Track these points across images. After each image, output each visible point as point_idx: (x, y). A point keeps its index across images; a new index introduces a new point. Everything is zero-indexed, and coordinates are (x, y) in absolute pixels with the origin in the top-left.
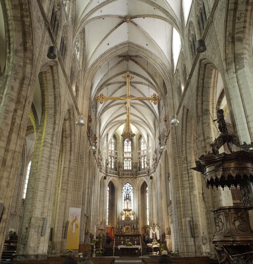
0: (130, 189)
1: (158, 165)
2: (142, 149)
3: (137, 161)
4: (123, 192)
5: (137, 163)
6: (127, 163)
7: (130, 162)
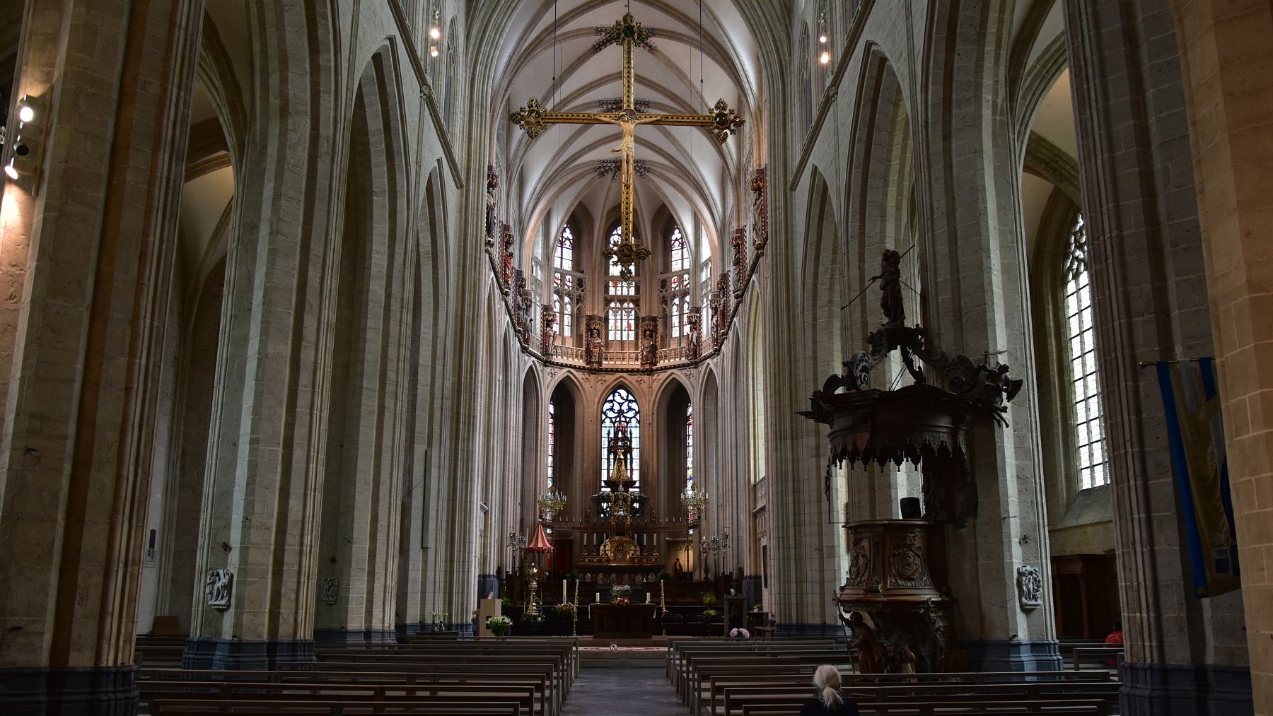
0: (630, 409)
1: (731, 333)
2: (676, 266)
4: (603, 422)
5: (654, 319)
6: (619, 317)
7: (628, 316)
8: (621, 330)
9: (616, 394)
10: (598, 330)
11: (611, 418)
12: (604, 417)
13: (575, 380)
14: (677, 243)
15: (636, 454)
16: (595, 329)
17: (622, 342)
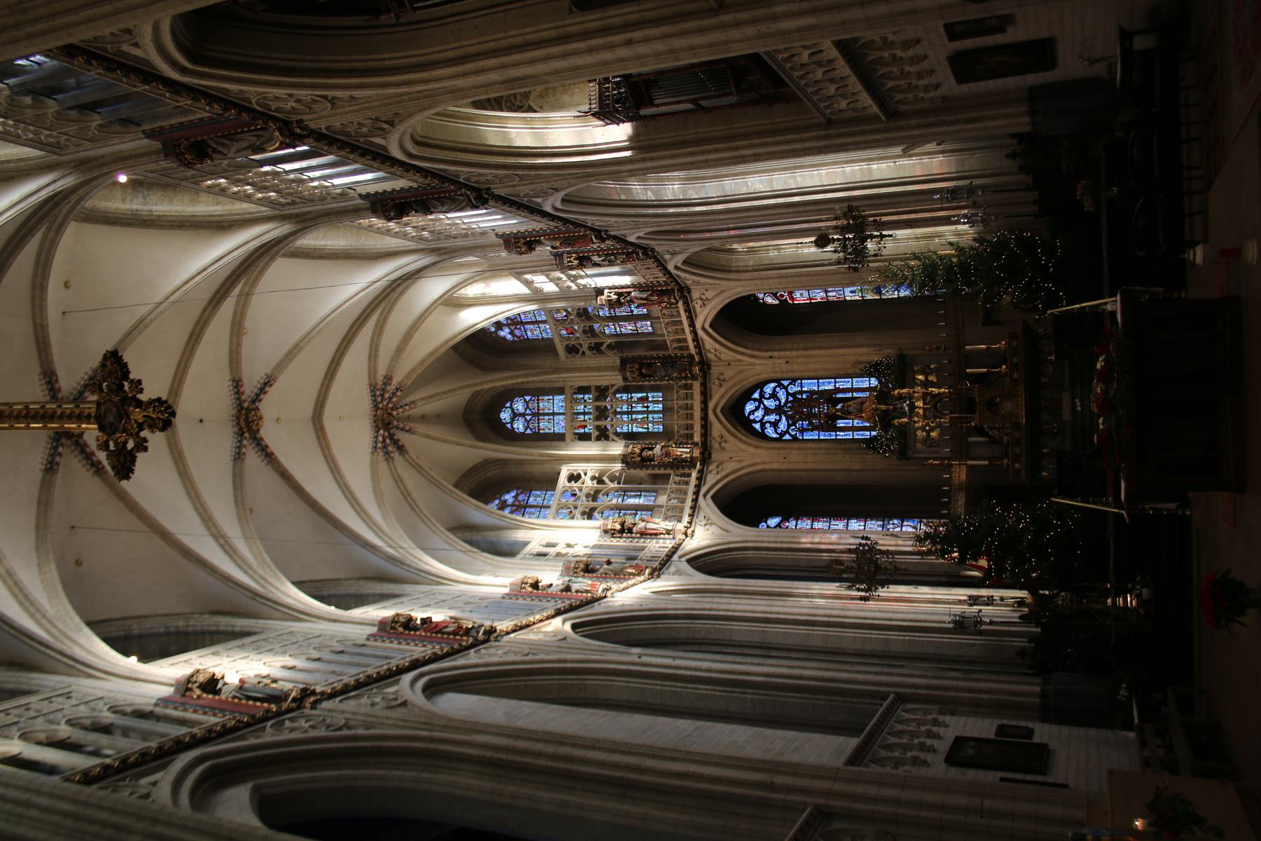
3: (614, 359)
4: (795, 438)
5: (624, 362)
6: (625, 417)
8: (648, 412)
9: (752, 417)
10: (642, 450)
11: (789, 426)
12: (787, 437)
13: (719, 486)
14: (517, 332)
15: (828, 385)
16: (640, 455)
17: (664, 411)
